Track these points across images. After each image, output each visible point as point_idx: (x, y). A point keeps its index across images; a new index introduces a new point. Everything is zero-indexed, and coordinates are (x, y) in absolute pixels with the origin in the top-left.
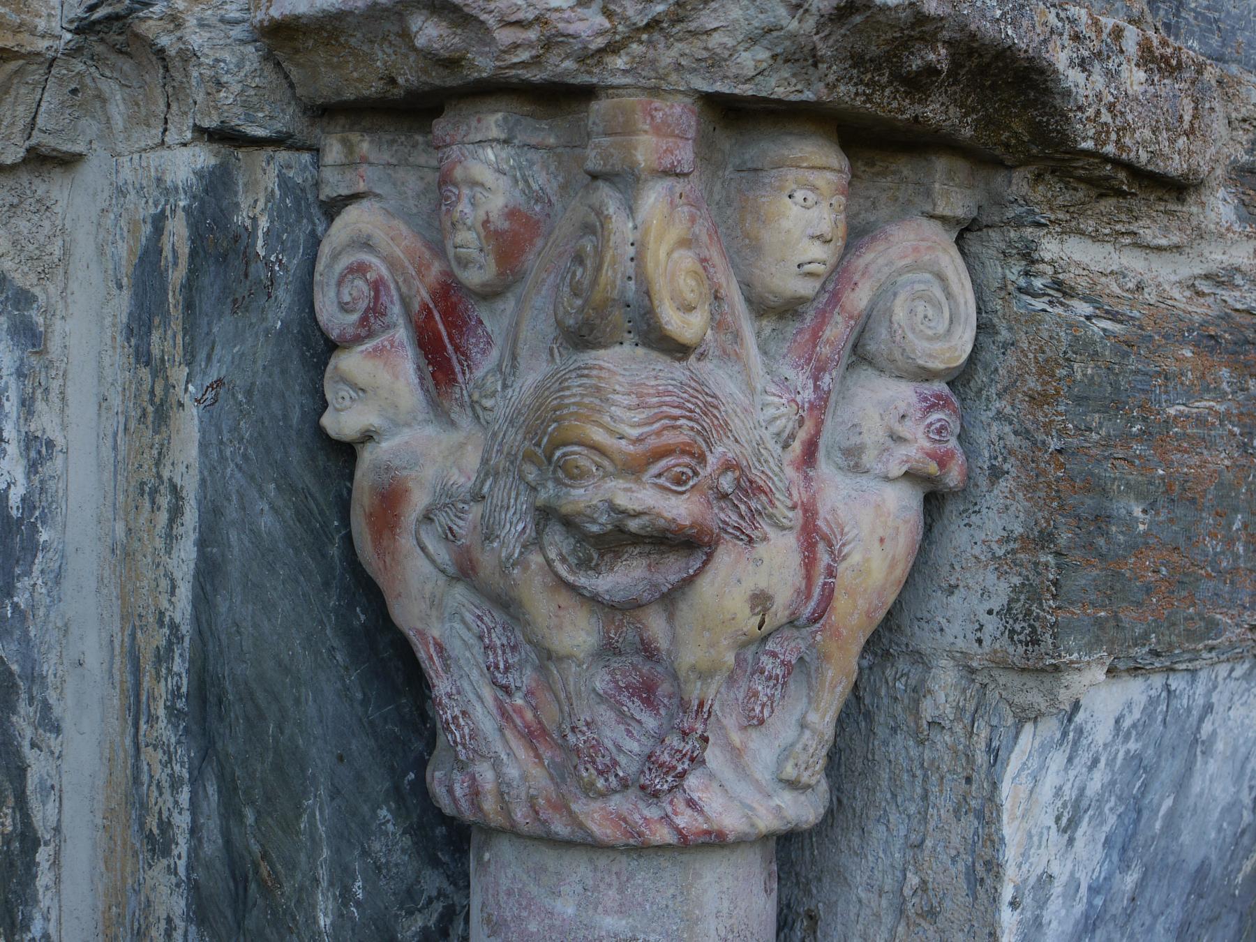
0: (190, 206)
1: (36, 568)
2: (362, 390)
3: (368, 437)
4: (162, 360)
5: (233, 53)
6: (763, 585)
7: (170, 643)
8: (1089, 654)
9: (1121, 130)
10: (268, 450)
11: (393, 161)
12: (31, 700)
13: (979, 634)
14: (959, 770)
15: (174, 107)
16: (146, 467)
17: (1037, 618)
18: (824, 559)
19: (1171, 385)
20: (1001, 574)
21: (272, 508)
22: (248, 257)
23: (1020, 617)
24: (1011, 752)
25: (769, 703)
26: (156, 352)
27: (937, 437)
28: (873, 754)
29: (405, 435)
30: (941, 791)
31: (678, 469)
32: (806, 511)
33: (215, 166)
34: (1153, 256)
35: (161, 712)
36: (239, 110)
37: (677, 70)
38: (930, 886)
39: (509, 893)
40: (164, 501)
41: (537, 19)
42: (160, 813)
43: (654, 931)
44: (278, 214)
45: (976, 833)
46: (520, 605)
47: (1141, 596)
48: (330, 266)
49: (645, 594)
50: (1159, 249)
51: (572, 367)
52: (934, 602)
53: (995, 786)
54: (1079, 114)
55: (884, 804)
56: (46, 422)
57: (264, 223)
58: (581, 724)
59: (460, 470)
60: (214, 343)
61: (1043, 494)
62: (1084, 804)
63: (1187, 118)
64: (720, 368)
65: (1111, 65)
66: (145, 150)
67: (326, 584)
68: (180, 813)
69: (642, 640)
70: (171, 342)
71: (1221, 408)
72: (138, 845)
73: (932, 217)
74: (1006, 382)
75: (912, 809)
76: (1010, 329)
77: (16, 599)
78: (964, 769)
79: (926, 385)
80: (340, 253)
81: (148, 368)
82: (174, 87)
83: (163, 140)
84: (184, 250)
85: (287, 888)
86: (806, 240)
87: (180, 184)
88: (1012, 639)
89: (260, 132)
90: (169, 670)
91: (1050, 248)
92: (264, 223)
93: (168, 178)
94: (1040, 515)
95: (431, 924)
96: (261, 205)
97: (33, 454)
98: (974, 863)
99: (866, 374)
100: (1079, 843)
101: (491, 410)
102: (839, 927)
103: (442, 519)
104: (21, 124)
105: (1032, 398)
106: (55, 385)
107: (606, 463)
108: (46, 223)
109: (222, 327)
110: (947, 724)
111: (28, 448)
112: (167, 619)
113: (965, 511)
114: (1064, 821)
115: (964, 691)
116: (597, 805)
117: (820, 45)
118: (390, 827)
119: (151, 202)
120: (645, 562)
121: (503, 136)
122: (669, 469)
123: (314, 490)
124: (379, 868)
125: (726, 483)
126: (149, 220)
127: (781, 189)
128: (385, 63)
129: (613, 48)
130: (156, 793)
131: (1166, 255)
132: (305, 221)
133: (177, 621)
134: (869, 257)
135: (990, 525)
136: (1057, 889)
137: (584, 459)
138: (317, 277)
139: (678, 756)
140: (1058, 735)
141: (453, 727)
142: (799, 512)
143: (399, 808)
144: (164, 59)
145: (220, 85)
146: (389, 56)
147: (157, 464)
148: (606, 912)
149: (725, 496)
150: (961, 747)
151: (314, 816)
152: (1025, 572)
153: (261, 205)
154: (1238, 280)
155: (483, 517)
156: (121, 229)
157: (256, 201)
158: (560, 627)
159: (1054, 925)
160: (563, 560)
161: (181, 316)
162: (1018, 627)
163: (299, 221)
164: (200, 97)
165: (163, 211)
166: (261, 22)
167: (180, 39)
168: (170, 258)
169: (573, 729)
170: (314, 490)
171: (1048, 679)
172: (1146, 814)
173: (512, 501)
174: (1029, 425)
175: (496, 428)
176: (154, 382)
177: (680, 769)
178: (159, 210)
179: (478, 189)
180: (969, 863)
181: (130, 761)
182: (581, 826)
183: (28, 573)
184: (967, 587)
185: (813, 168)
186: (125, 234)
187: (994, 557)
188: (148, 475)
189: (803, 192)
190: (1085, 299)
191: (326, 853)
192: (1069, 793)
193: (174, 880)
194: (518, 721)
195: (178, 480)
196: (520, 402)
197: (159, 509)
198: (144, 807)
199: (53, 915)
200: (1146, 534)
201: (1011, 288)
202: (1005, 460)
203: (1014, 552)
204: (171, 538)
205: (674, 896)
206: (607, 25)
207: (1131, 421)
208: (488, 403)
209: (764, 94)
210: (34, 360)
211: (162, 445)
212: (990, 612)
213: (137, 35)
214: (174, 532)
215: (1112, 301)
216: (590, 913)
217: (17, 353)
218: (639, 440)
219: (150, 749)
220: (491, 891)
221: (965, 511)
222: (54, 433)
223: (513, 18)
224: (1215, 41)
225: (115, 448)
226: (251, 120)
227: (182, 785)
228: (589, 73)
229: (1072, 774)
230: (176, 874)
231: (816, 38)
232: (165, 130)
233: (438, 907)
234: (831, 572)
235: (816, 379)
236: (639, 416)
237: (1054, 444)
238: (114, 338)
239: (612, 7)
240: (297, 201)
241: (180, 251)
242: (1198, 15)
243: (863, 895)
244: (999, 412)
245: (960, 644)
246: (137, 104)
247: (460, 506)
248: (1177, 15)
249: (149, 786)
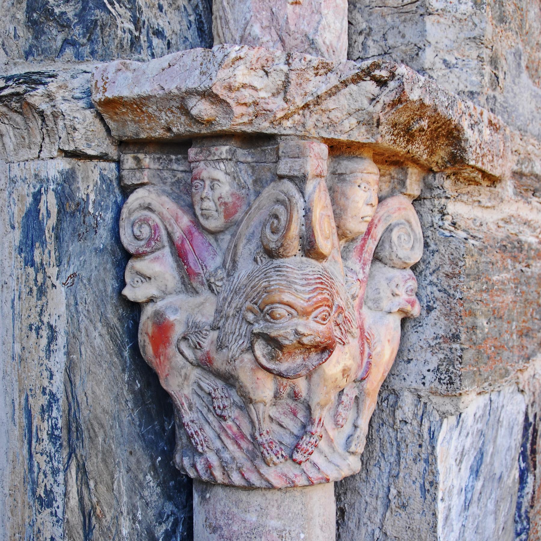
0: (57, 188)
2: (150, 278)
3: (151, 300)
4: (42, 264)
5: (81, 113)
7: (50, 403)
8: (471, 387)
9: (483, 156)
10: (98, 306)
11: (160, 168)
13: (423, 381)
14: (415, 441)
15: (47, 140)
16: (32, 316)
17: (452, 372)
18: (367, 350)
19: (494, 267)
20: (433, 353)
23: (444, 372)
26: (37, 260)
28: (372, 436)
29: (169, 299)
30: (407, 451)
31: (324, 313)
32: (361, 329)
33: (69, 169)
34: (485, 211)
35: (45, 437)
36: (84, 142)
38: (402, 494)
39: (222, 513)
40: (45, 333)
41: (254, 102)
42: (45, 486)
44: (99, 192)
45: (425, 469)
46: (237, 379)
47: (486, 360)
50: (487, 207)
51: (271, 267)
52: (400, 367)
53: (434, 448)
55: (377, 458)
57: (92, 197)
58: (264, 433)
59: (203, 315)
60: (70, 255)
61: (454, 318)
62: (464, 453)
63: (502, 150)
65: (480, 127)
66: (27, 160)
67: (124, 370)
68: (58, 486)
69: (295, 392)
70: (48, 255)
71: (508, 276)
72: (32, 503)
74: (434, 268)
75: (392, 460)
76: (436, 244)
78: (418, 441)
80: (134, 211)
81: (33, 268)
82: (47, 130)
83: (39, 156)
84: (54, 210)
86: (365, 205)
87: (50, 178)
88: (440, 382)
89: (90, 152)
90: (50, 416)
93: (43, 175)
94: (452, 327)
95: (169, 528)
96: (91, 188)
98: (424, 483)
99: (379, 265)
100: (462, 470)
101: (221, 287)
102: (356, 514)
103: (193, 339)
105: (447, 275)
107: (293, 311)
109: (73, 247)
110: (409, 421)
112: (47, 391)
113: (415, 325)
115: (416, 406)
117: (381, 118)
118: (151, 484)
119: (31, 186)
120: (302, 356)
121: (229, 157)
123: (118, 325)
124: (147, 504)
126: (31, 195)
127: (355, 182)
128: (166, 121)
129: (286, 117)
130: (43, 477)
131: (489, 210)
132: (112, 196)
133: (54, 392)
135: (428, 332)
137: (281, 310)
138: (121, 223)
140: (456, 423)
141: (195, 436)
143: (154, 475)
144: (43, 116)
145: (75, 129)
146: (169, 117)
147: (40, 315)
148: (271, 519)
150: (416, 431)
152: (445, 352)
153: (91, 188)
154: (513, 221)
155: (218, 337)
156: (13, 199)
157: (88, 186)
158: (258, 388)
159: (455, 507)
160: (264, 356)
161: (53, 243)
162: (443, 377)
163: (109, 196)
164: (63, 135)
165: (40, 191)
166: (100, 99)
167: (54, 106)
168: (45, 214)
169: (261, 435)
170: (118, 325)
171: (455, 399)
172: (484, 454)
173: (237, 330)
174: (446, 287)
175: (226, 295)
176: (36, 275)
177: (310, 450)
178: (37, 189)
179: (216, 182)
180: (422, 483)
181: (26, 462)
184: (417, 360)
186: (16, 201)
187: (430, 346)
188: (34, 320)
191: (125, 499)
192: (460, 449)
193: (55, 519)
194: (229, 432)
195: (53, 323)
196: (239, 283)
197: (41, 337)
198: (35, 483)
200: (487, 334)
201: (435, 226)
202: (434, 302)
203: (439, 343)
204: (49, 351)
207: (483, 284)
208: (219, 284)
211: (43, 306)
212: (429, 371)
213: (28, 104)
214: (52, 348)
215: (473, 231)
216: (264, 519)
219: (39, 455)
220: (211, 512)
221: (415, 325)
223: (243, 102)
224: (506, 116)
225: (13, 307)
226: (89, 146)
227: (59, 472)
229: (460, 439)
230: (56, 516)
232: (41, 151)
233: (172, 519)
234: (370, 356)
236: (308, 289)
237: (458, 296)
238: (10, 253)
239: (288, 97)
240: (108, 186)
241: (51, 211)
242: (501, 105)
243: (368, 500)
244: (431, 281)
245: (414, 385)
246: (24, 138)
247: (204, 332)
248: (494, 105)
249: (38, 473)
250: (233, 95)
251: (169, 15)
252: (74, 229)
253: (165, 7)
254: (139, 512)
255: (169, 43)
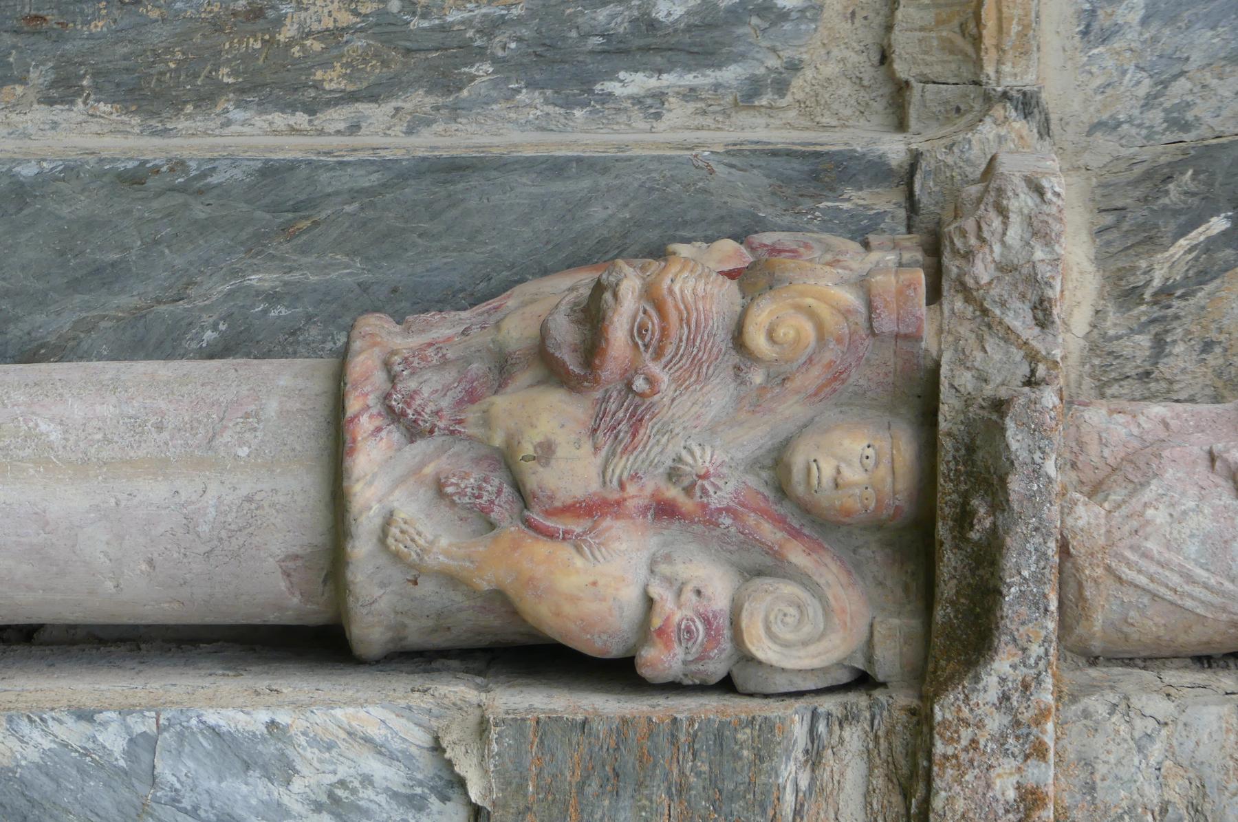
1: (550, 109)
6: (560, 452)
12: (437, 109)
18: (577, 527)
21: (611, 216)
22: (816, 197)
24: (408, 719)
25: (460, 490)
27: (683, 627)
31: (650, 326)
32: (619, 503)
36: (933, 166)
37: (955, 340)
43: (265, 435)
48: (811, 238)
49: (553, 341)
54: (961, 697)
56: (677, 113)
64: (731, 397)
73: (871, 626)
77: (524, 91)
79: (727, 623)
85: (286, 246)
91: (853, 737)
92: (846, 206)
96: (861, 202)
97: (649, 101)
104: (927, 71)
106: (708, 121)
108: (848, 112)
109: (757, 177)
111: (653, 96)
114: (340, 793)
116: (378, 363)
122: (650, 317)
124: (293, 334)
125: (640, 384)
129: (968, 298)
134: (834, 567)
136: (277, 791)
139: (419, 409)
142: (615, 496)
148: (281, 403)
149: (629, 386)
151: (345, 268)
159: (244, 789)
177: (410, 412)
182: (360, 353)
183: (547, 102)
185: (893, 460)
189: (873, 455)
190: (813, 780)
191: (313, 279)
199: (247, 129)
205: (293, 450)
206: (983, 282)
209: (942, 397)
210: (729, 99)
217: (735, 83)
218: (671, 291)
222: (669, 119)
228: (950, 288)
231: (980, 400)
235: (728, 510)
250: (990, 209)
251: (1200, 370)
252: (788, 181)
253: (1210, 358)
254: (284, 312)
255: (1147, 374)
